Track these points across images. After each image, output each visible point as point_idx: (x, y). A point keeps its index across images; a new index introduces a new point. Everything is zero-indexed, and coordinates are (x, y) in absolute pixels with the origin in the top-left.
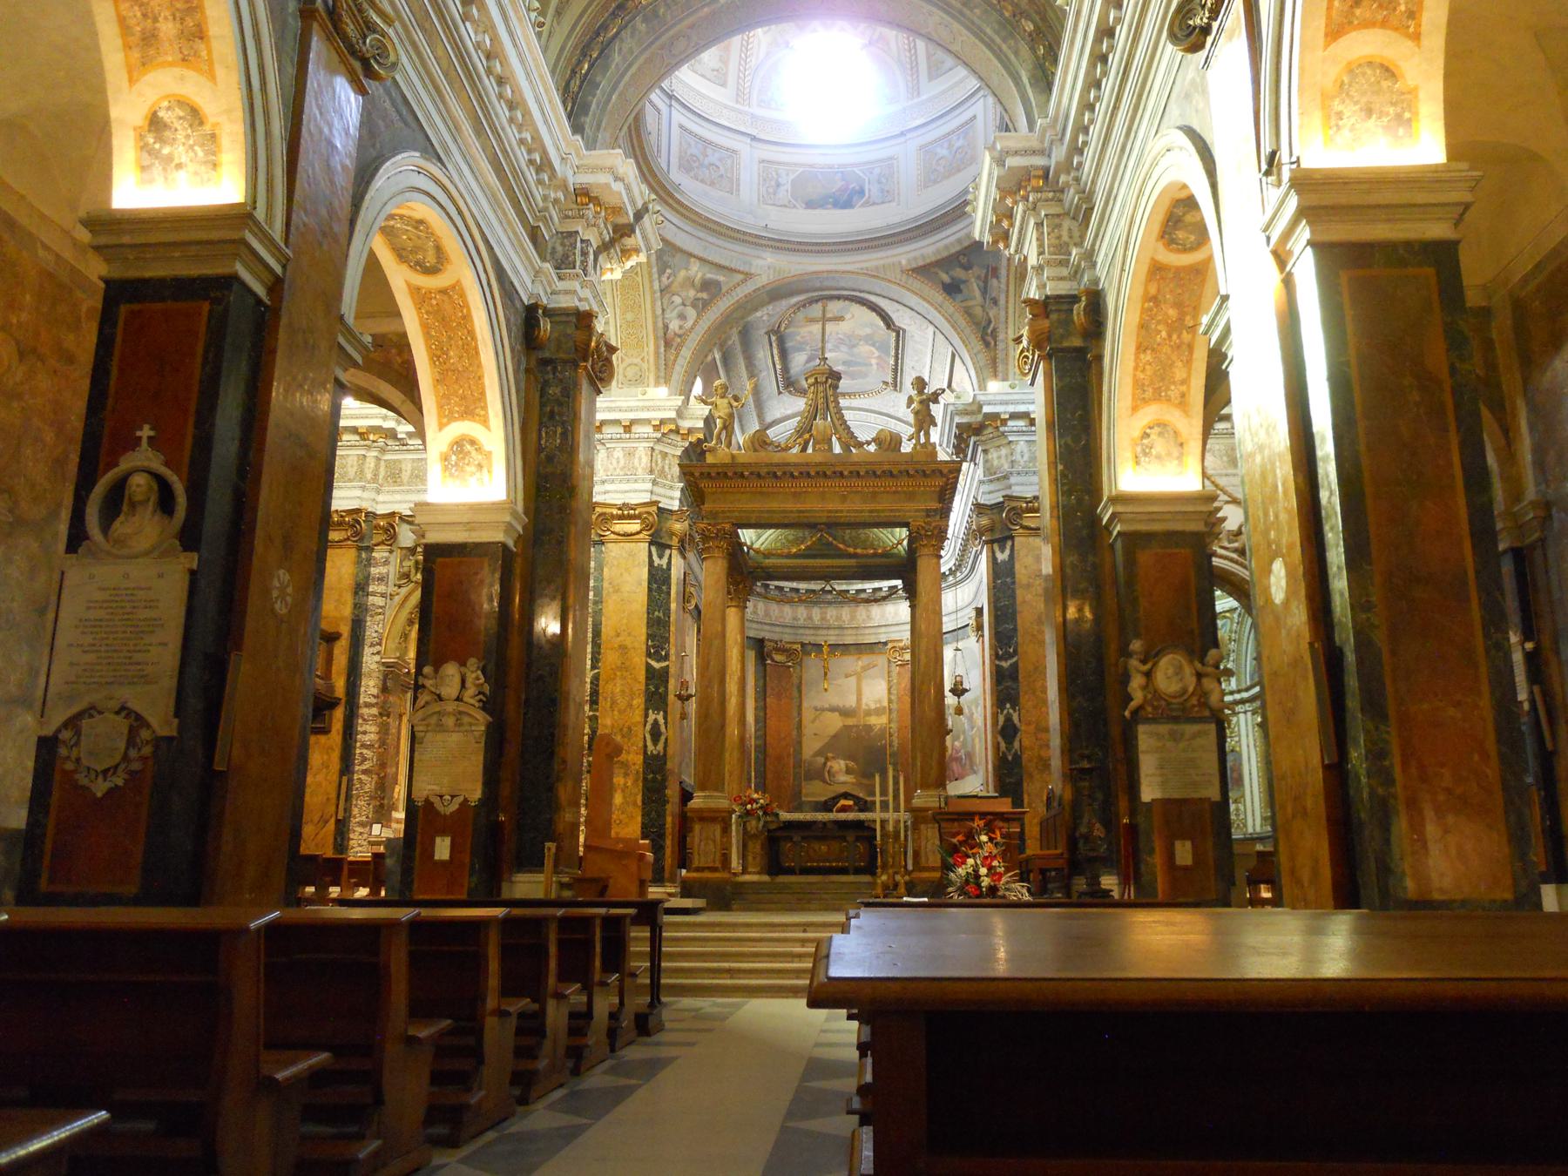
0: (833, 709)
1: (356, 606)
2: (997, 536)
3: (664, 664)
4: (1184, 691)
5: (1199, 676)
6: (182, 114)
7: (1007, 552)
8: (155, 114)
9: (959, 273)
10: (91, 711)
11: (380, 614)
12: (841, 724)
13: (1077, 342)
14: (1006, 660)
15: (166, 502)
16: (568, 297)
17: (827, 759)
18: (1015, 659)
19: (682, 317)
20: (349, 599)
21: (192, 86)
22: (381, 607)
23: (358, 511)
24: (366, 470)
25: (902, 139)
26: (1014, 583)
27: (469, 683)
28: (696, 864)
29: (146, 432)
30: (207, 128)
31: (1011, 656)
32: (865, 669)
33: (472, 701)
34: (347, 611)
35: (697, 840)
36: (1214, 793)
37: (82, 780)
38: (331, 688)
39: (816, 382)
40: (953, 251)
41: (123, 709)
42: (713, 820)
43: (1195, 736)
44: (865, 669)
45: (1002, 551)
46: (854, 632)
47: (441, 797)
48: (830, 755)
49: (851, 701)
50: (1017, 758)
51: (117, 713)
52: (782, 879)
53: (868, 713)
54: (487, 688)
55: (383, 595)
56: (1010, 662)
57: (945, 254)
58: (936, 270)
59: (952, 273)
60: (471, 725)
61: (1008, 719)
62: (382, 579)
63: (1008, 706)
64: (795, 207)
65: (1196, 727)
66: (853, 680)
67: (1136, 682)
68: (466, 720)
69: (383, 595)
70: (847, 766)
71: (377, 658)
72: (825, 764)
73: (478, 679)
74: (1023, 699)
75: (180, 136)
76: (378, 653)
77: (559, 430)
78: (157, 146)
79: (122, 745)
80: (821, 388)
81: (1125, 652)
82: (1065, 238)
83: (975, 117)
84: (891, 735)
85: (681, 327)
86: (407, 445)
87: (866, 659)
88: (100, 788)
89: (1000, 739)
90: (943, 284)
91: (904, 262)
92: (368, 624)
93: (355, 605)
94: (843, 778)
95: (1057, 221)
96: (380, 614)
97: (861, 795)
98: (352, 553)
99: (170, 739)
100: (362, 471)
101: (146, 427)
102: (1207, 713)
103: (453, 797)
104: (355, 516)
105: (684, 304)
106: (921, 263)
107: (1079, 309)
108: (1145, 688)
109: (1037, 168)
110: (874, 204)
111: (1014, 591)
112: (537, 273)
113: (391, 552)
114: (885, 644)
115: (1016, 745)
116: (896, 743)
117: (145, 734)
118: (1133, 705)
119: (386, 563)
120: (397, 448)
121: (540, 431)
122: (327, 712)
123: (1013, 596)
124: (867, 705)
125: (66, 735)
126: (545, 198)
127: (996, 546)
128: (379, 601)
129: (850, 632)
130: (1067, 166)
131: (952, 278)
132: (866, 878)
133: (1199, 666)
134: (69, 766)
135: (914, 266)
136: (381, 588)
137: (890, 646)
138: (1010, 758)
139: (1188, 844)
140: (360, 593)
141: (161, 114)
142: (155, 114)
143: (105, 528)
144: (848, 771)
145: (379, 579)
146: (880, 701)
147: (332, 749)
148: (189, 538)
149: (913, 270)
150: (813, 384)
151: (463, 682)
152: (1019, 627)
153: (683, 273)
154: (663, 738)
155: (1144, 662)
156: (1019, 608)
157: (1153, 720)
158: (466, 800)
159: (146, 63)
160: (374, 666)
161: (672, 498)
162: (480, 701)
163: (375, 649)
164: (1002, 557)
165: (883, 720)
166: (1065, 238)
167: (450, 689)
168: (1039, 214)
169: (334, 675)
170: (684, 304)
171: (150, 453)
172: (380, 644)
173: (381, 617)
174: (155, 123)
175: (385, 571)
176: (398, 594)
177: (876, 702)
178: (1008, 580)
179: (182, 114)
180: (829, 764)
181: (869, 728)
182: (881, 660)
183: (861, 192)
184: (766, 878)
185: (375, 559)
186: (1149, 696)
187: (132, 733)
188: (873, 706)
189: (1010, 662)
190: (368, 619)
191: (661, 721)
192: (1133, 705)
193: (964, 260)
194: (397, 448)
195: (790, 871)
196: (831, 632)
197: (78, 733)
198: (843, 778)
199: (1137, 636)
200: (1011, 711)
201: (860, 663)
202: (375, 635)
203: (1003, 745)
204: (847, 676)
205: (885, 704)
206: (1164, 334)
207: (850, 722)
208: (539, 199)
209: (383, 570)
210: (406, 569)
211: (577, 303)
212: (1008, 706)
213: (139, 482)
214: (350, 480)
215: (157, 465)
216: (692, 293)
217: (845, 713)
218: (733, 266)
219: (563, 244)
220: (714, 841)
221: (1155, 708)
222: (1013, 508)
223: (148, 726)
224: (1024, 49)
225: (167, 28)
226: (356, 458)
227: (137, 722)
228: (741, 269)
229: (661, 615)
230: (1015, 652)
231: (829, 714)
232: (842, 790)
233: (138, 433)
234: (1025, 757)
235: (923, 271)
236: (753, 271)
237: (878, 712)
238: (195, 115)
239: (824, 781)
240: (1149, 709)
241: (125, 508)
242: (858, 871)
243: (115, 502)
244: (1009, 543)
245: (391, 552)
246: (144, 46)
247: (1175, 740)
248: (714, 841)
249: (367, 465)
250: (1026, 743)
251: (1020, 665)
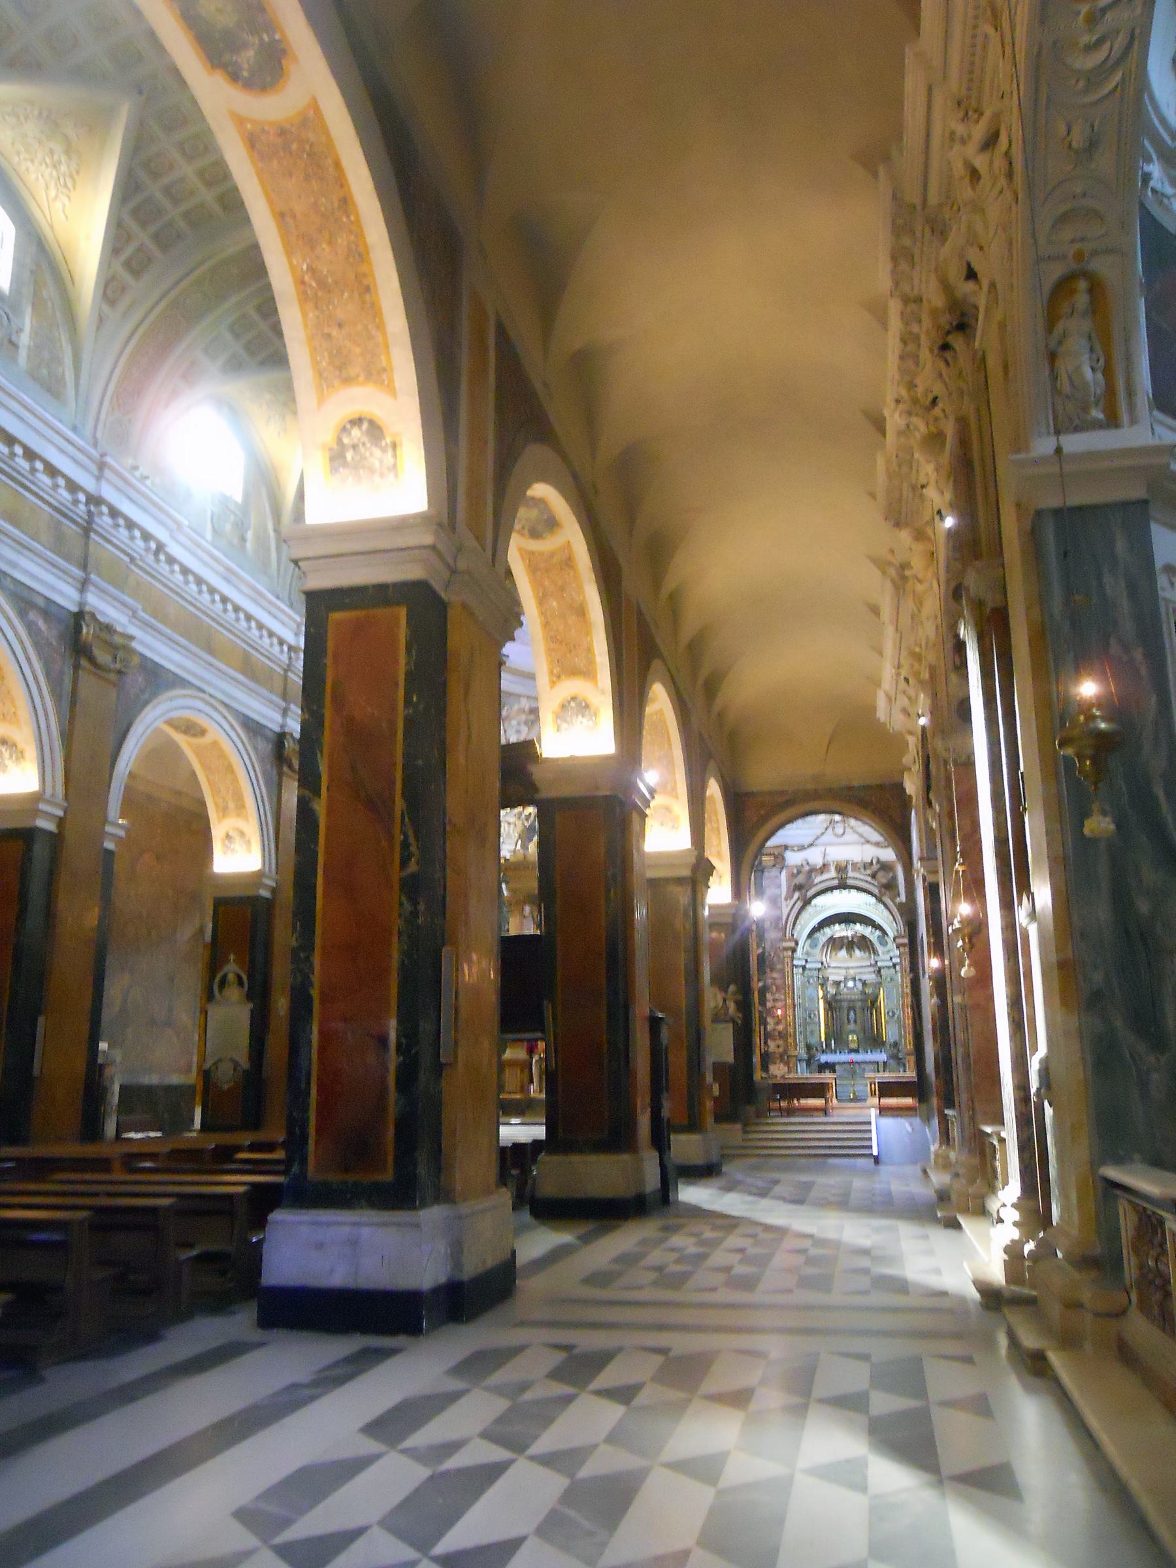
5: (725, 1001)
8: (228, 834)
10: (220, 1060)
15: (240, 982)
19: (518, 732)
21: (241, 824)
28: (507, 1089)
29: (232, 957)
30: (247, 839)
41: (232, 1060)
75: (237, 841)
88: (226, 1087)
117: (239, 1068)
142: (228, 834)
153: (516, 707)
159: (224, 816)
174: (228, 836)
197: (217, 1068)
213: (231, 977)
216: (523, 717)
225: (231, 805)
227: (236, 1065)
238: (242, 834)
241: (227, 985)
243: (223, 983)
246: (224, 811)
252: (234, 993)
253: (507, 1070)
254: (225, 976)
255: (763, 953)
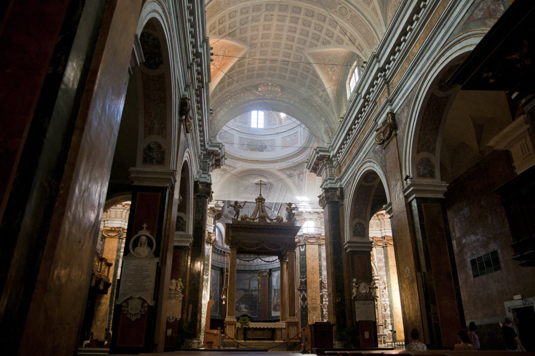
0: (242, 289)
2: (301, 244)
3: (207, 277)
4: (366, 292)
5: (370, 288)
6: (156, 146)
7: (304, 249)
9: (292, 172)
10: (131, 298)
12: (244, 294)
13: (337, 200)
14: (303, 279)
15: (150, 244)
16: (205, 179)
17: (240, 304)
18: (306, 279)
20: (115, 253)
23: (120, 228)
24: (123, 216)
25: (277, 135)
26: (306, 257)
27: (179, 285)
29: (145, 226)
31: (305, 278)
32: (251, 277)
33: (179, 290)
34: (115, 257)
35: (227, 330)
36: (375, 320)
37: (128, 316)
38: (109, 280)
39: (259, 201)
40: (291, 166)
41: (140, 298)
42: (233, 324)
43: (369, 304)
44: (251, 277)
45: (302, 249)
46: (249, 266)
47: (169, 317)
48: (240, 303)
49: (247, 287)
50: (306, 307)
51: (138, 299)
52: (247, 341)
53: (252, 291)
54: (183, 287)
56: (304, 280)
57: (289, 167)
58: (286, 170)
59: (290, 172)
60: (178, 297)
61: (304, 296)
63: (304, 292)
64: (248, 150)
65: (369, 302)
66: (248, 281)
67: (354, 290)
68: (177, 296)
70: (245, 306)
72: (239, 306)
73: (181, 284)
74: (308, 290)
77: (201, 215)
78: (149, 153)
79: (140, 307)
80: (260, 203)
81: (350, 282)
82: (333, 173)
83: (298, 132)
84: (259, 297)
85: (216, 181)
87: (252, 275)
88: (133, 319)
89: (301, 301)
90: (288, 174)
91: (277, 168)
94: (244, 310)
95: (331, 168)
97: (249, 315)
99: (152, 306)
100: (122, 216)
101: (145, 224)
102: (372, 298)
103: (173, 317)
104: (119, 229)
105: (217, 175)
106: (282, 168)
107: (338, 192)
108: (357, 291)
109: (327, 155)
110: (269, 151)
111: (306, 260)
112: (198, 172)
114: (258, 270)
115: (306, 303)
116: (260, 300)
118: (354, 295)
121: (196, 215)
123: (306, 261)
124: (252, 288)
125: (124, 304)
126: (201, 153)
127: (301, 247)
129: (247, 266)
130: (335, 156)
131: (290, 173)
132: (271, 342)
133: (369, 286)
134: (125, 313)
135: (280, 169)
137: (259, 271)
138: (304, 307)
139: (368, 333)
141: (151, 145)
143: (133, 250)
144: (246, 308)
146: (256, 287)
148: (156, 254)
149: (280, 170)
150: (258, 202)
151: (177, 285)
152: (307, 270)
154: (206, 299)
155: (356, 284)
156: (307, 265)
157: (359, 300)
158: (176, 319)
161: (211, 229)
162: (181, 290)
164: (302, 250)
165: (257, 293)
166: (333, 173)
167: (173, 288)
168: (326, 166)
169: (110, 276)
170: (217, 175)
171: (146, 231)
177: (254, 287)
178: (304, 256)
179: (156, 146)
180: (240, 306)
181: (252, 295)
182: (256, 275)
183: (266, 148)
184: (243, 341)
186: (358, 293)
187: (143, 304)
188: (254, 289)
189: (304, 280)
191: (206, 294)
192: (354, 295)
193: (294, 168)
195: (249, 339)
196: (242, 266)
197: (128, 304)
198: (244, 310)
199: (355, 278)
200: (304, 293)
201: (250, 276)
203: (302, 303)
204: (246, 279)
205: (257, 288)
206: (361, 201)
207: (247, 293)
208: (200, 153)
211: (207, 181)
212: (304, 292)
213: (144, 238)
214: (118, 218)
215: (148, 234)
217: (245, 290)
218: (231, 165)
219: (203, 164)
220: (232, 331)
221: (359, 297)
222: (306, 237)
223: (146, 302)
224: (323, 126)
225: (156, 126)
226: (120, 212)
227: (145, 301)
228: (233, 166)
229: (207, 262)
230: (306, 277)
231: (241, 290)
232: (244, 313)
233: (143, 226)
234: (308, 307)
235: (282, 170)
236: (236, 167)
237: (255, 290)
239: (239, 311)
240: (358, 297)
241: (139, 244)
242: (269, 339)
244: (304, 246)
247: (364, 305)
248: (232, 331)
249: (123, 214)
250: (309, 302)
251: (307, 280)
252: (144, 250)
253: (228, 326)
254: (138, 238)
255: (322, 280)
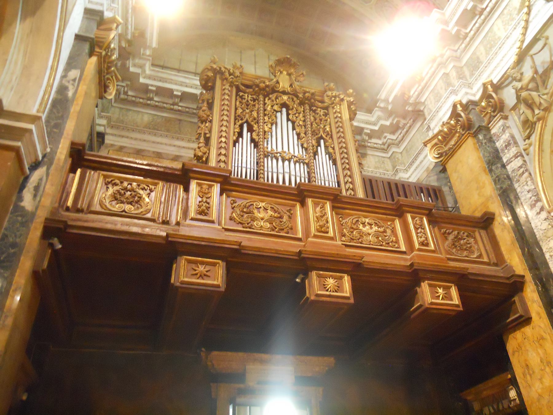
1: (497, 180)
11: (523, 173)
22: (521, 167)
55: (516, 157)
62: (508, 145)
69: (516, 157)
71: (544, 215)
76: (542, 209)
86: (467, 35)
92: (518, 190)
93: (495, 181)
96: (523, 173)
98: (470, 143)
113: (506, 118)
119: (505, 128)
120: (463, 46)
122: (516, 299)
128: (518, 162)
136: (513, 150)
140: (493, 168)
145: (506, 146)
147: (542, 338)
160: (545, 225)
163: (537, 209)
169: (506, 256)
172: (539, 200)
173: (526, 174)
175: (508, 135)
176: (530, 145)
185: (495, 134)
190: (516, 185)
194: (463, 46)
202: (530, 195)
209: (506, 136)
210: (522, 118)
245: (506, 118)
